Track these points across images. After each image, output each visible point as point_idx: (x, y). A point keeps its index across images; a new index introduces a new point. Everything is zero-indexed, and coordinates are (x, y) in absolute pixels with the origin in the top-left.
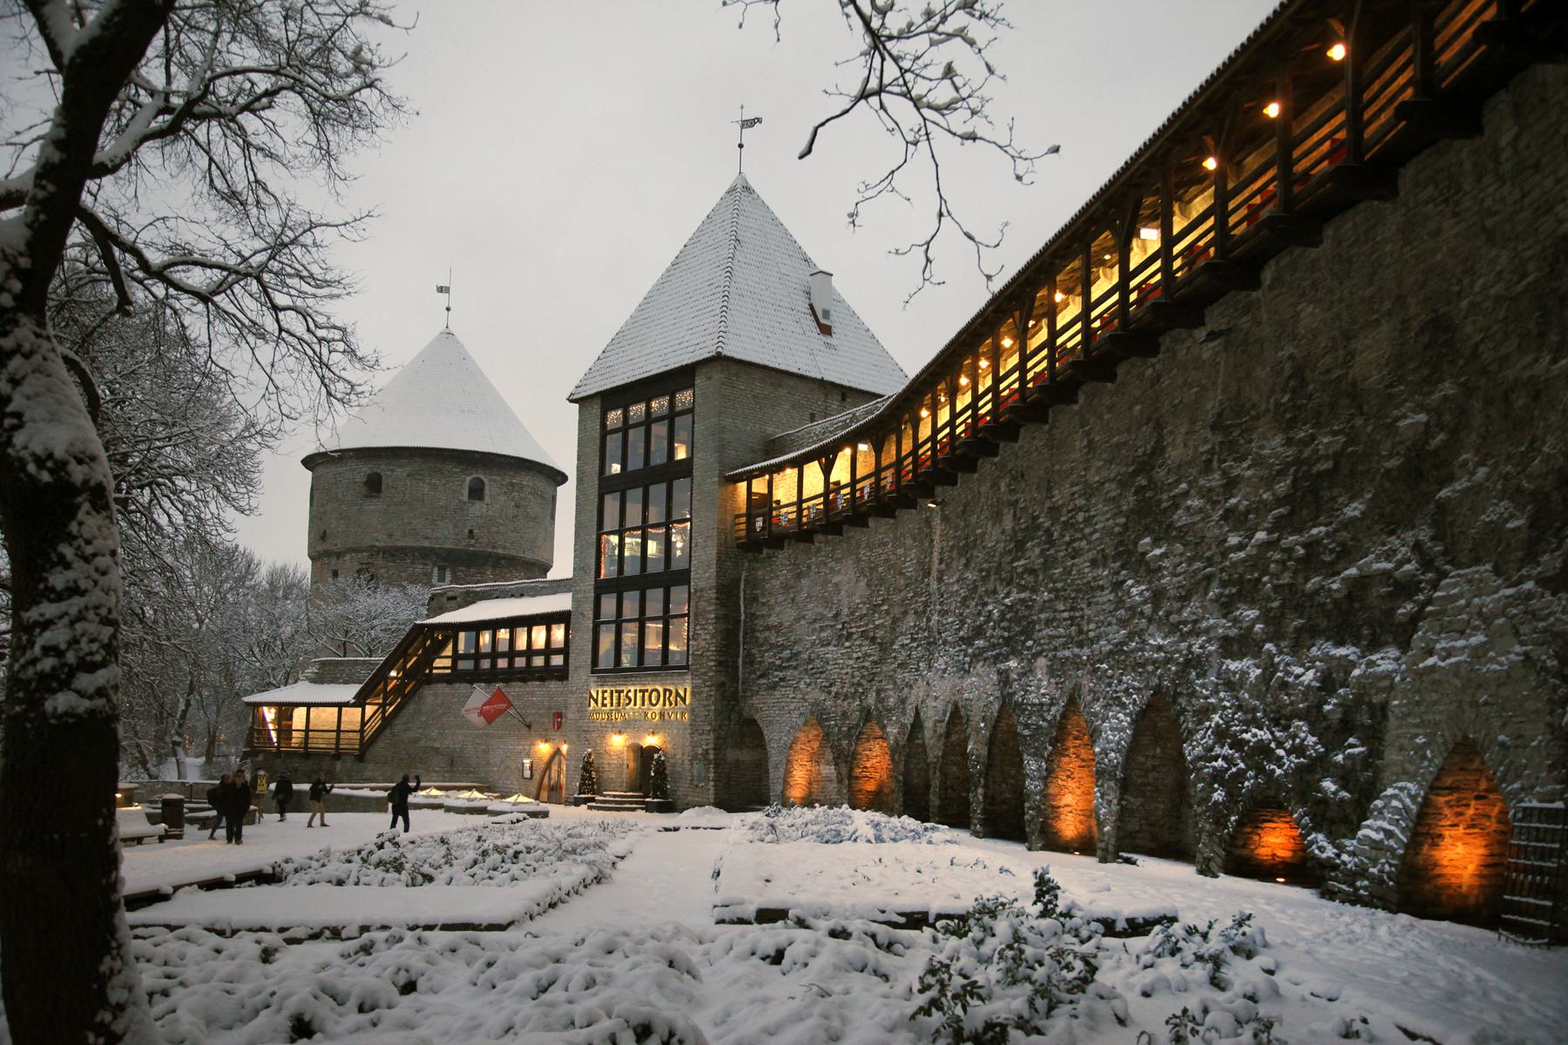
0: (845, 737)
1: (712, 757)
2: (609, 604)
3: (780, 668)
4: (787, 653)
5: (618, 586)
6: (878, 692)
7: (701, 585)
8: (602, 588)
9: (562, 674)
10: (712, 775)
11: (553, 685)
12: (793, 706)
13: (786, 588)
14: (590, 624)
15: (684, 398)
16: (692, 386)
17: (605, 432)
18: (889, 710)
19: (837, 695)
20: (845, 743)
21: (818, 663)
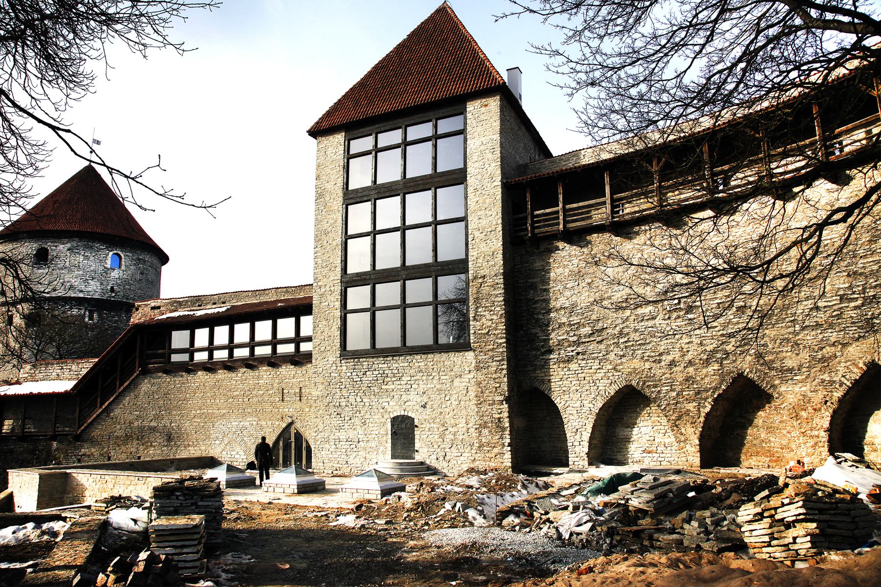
0: (689, 401)
1: (507, 425)
2: (359, 297)
3: (578, 343)
4: (587, 330)
5: (374, 278)
6: (759, 356)
7: (482, 273)
8: (350, 281)
9: (300, 359)
10: (508, 441)
11: (287, 370)
12: (599, 376)
13: (579, 275)
14: (338, 314)
15: (445, 126)
16: (462, 112)
17: (349, 156)
18: (791, 370)
19: (673, 364)
20: (691, 406)
21: (633, 336)
